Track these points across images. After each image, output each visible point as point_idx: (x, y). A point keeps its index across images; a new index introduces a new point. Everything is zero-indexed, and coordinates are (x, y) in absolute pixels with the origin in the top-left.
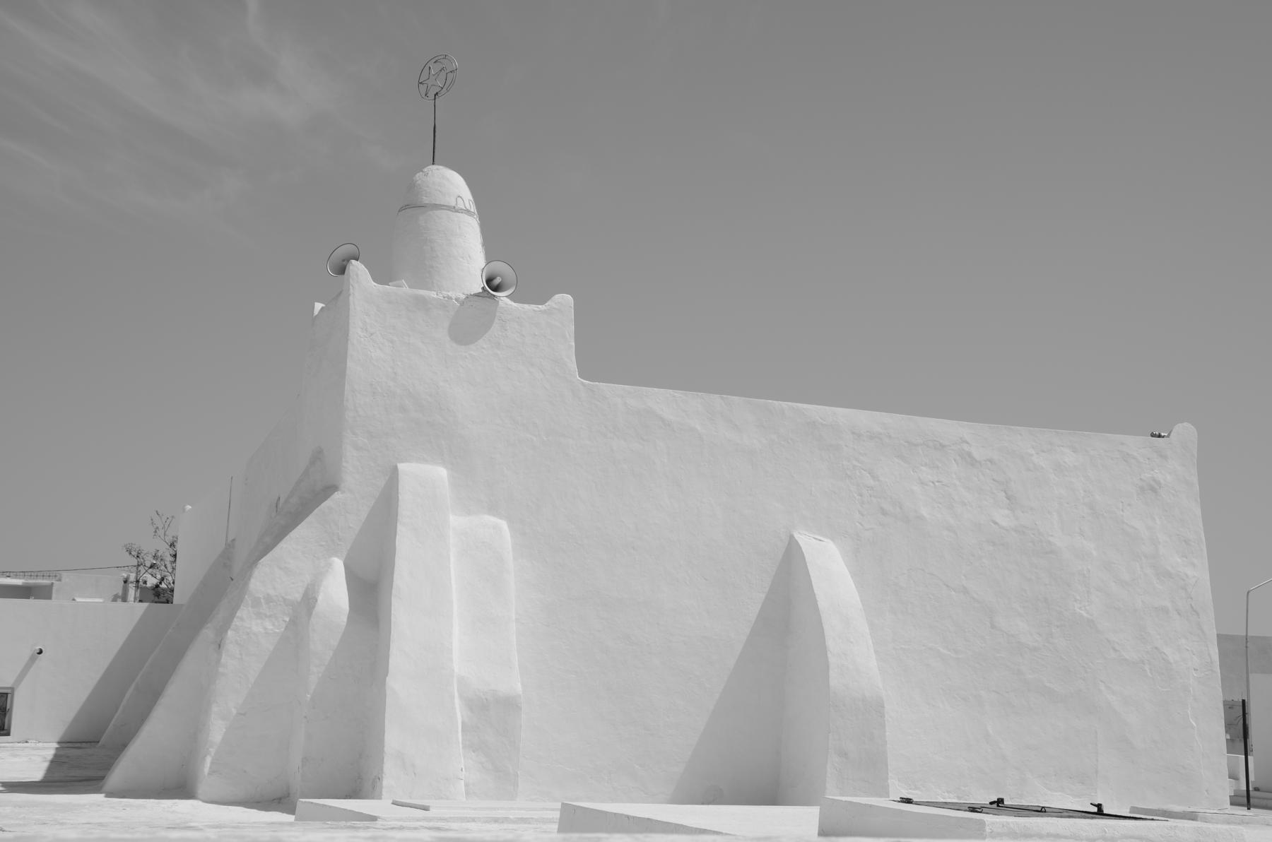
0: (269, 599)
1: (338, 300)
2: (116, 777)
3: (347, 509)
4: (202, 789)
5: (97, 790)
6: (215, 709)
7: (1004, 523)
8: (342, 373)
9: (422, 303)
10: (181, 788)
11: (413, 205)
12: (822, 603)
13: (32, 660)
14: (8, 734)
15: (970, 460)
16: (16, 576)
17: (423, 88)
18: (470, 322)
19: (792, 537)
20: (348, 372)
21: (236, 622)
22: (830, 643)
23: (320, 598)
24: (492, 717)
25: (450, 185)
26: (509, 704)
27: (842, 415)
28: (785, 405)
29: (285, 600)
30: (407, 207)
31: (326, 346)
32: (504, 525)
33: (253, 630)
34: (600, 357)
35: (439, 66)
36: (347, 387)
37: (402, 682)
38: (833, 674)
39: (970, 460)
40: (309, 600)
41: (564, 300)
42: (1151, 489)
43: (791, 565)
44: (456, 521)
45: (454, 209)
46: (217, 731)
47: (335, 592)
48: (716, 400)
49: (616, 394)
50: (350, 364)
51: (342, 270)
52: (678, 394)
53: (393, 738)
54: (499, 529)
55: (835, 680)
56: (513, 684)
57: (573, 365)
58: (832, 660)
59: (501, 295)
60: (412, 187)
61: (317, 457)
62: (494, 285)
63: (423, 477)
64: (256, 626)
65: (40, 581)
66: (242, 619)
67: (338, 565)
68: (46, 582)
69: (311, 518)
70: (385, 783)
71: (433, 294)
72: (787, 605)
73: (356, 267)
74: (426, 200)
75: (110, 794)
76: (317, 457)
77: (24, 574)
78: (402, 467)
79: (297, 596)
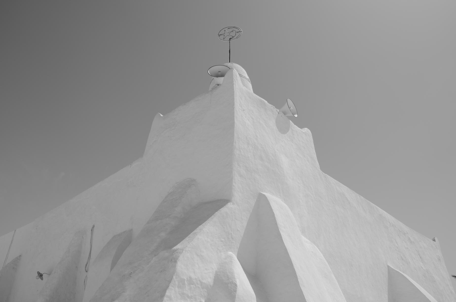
0: (191, 282)
3: (236, 215)
8: (232, 125)
17: (222, 37)
19: (388, 267)
20: (235, 126)
23: (238, 283)
27: (385, 213)
29: (201, 283)
35: (231, 30)
36: (235, 135)
50: (235, 121)
52: (349, 189)
63: (277, 204)
66: (170, 299)
79: (209, 280)
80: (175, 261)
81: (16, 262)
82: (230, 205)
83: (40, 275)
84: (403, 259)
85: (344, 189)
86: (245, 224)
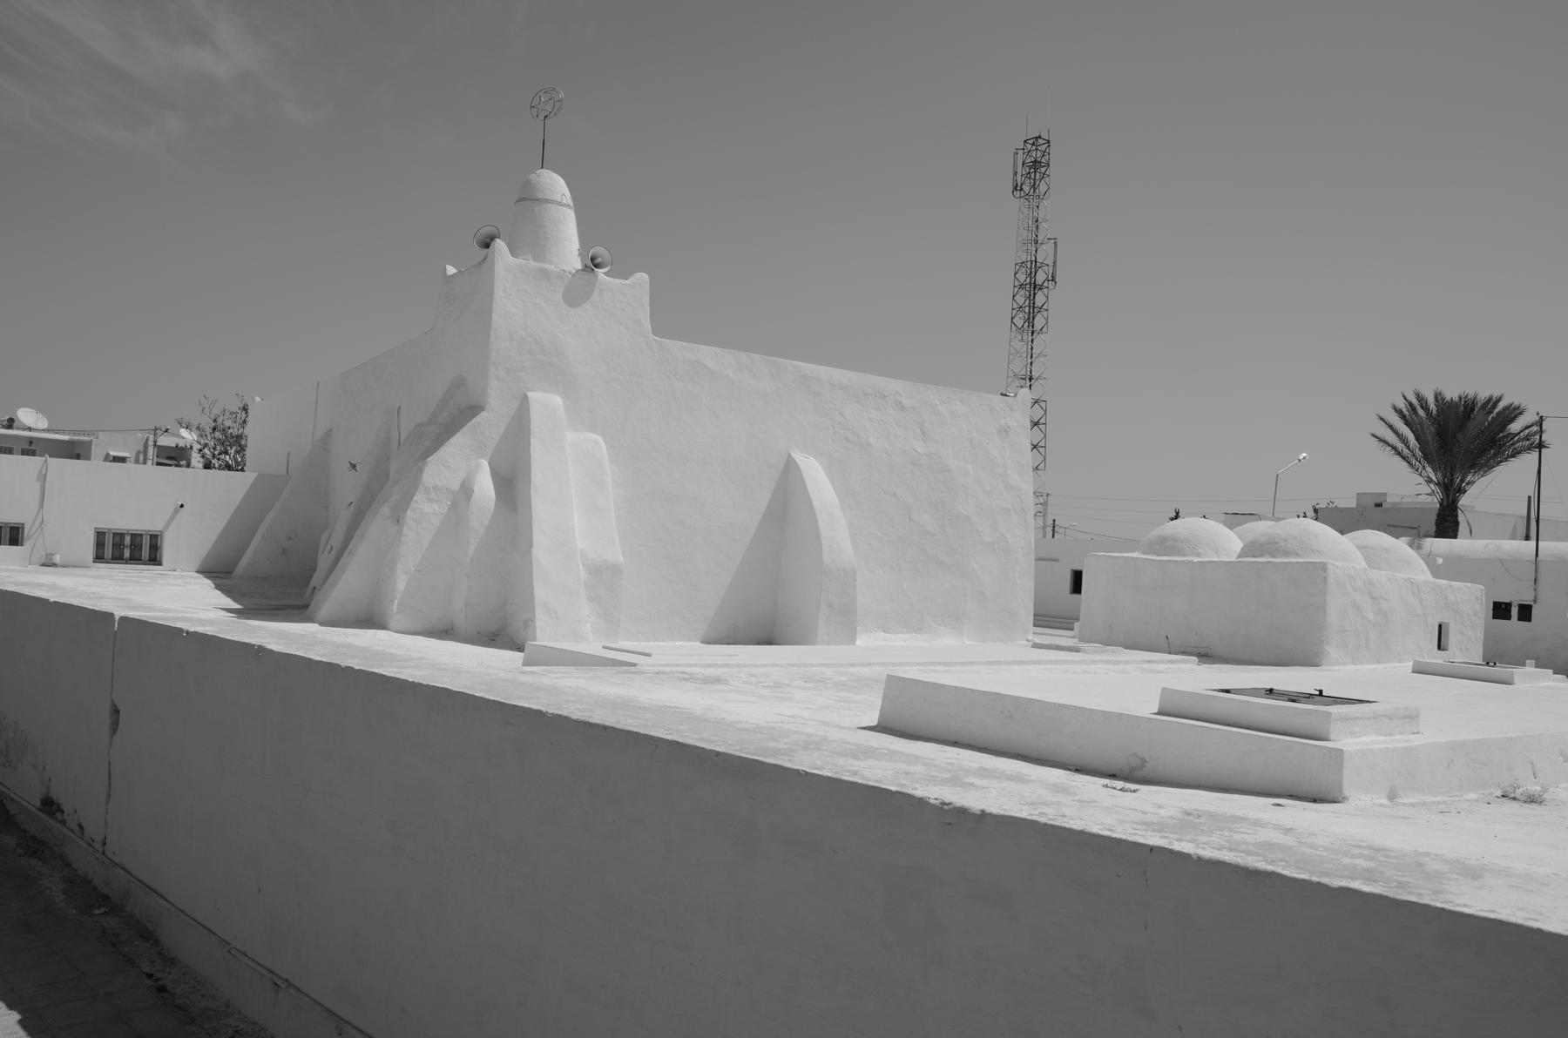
0: (436, 489)
1: (481, 269)
2: (326, 608)
3: (491, 423)
4: (393, 623)
5: (310, 620)
6: (400, 566)
7: (920, 450)
8: (488, 323)
9: (545, 274)
10: (371, 620)
11: (529, 198)
12: (815, 504)
13: (176, 511)
14: (160, 564)
15: (901, 407)
16: (63, 432)
17: (534, 111)
18: (577, 293)
21: (413, 504)
22: (822, 530)
23: (476, 489)
24: (603, 577)
25: (555, 185)
26: (615, 570)
27: (824, 371)
28: (788, 362)
30: (524, 199)
31: (470, 302)
32: (600, 439)
33: (426, 511)
34: (670, 319)
37: (542, 554)
38: (825, 552)
39: (901, 407)
40: (466, 490)
41: (642, 277)
42: (1005, 431)
43: (789, 475)
44: (571, 436)
45: (557, 203)
46: (401, 582)
47: (485, 486)
48: (743, 356)
49: (677, 347)
50: (494, 316)
51: (487, 246)
52: (718, 350)
53: (541, 593)
54: (595, 442)
55: (826, 556)
56: (615, 555)
57: (649, 327)
58: (824, 543)
59: (600, 272)
60: (527, 184)
61: (459, 383)
62: (594, 263)
63: (546, 403)
64: (427, 508)
65: (81, 438)
67: (485, 464)
68: (86, 438)
69: (465, 430)
70: (538, 624)
71: (553, 268)
72: (786, 504)
73: (500, 244)
74: (540, 196)
75: (322, 624)
76: (459, 383)
77: (69, 432)
78: (529, 394)
79: (456, 487)
80: (421, 471)
81: (325, 443)
82: (483, 414)
83: (354, 466)
84: (848, 440)
85: (708, 355)
86: (502, 429)
